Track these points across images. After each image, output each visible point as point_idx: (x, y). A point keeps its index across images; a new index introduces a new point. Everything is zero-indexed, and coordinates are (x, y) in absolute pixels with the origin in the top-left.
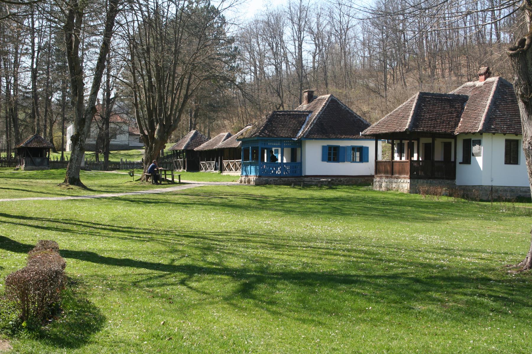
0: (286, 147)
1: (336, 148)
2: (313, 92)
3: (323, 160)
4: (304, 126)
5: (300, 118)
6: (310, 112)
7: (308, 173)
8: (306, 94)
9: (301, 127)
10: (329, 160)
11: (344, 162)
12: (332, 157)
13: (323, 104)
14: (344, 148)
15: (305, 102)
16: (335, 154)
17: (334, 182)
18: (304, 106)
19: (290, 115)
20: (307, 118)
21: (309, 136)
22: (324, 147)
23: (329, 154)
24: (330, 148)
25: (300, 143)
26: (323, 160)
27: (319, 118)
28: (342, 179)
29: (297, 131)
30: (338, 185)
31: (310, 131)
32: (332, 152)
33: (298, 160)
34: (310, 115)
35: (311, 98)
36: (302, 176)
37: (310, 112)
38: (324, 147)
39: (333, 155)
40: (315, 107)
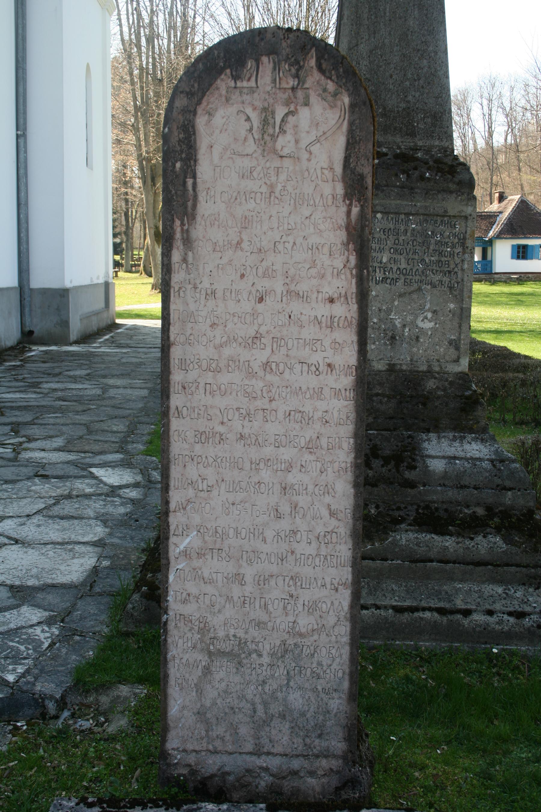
0: (478, 246)
1: (525, 247)
2: (503, 193)
3: (512, 258)
4: (494, 227)
5: (491, 218)
6: (501, 212)
7: (497, 271)
8: (497, 195)
9: (492, 227)
10: (518, 258)
11: (532, 259)
12: (521, 255)
13: (514, 205)
14: (532, 246)
15: (496, 202)
16: (523, 252)
17: (523, 278)
18: (495, 207)
19: (481, 216)
20: (498, 218)
21: (499, 236)
22: (513, 246)
23: (518, 252)
24: (519, 246)
25: (491, 242)
26: (512, 258)
27: (509, 219)
28: (530, 275)
29: (487, 231)
30: (526, 281)
31: (501, 231)
32: (521, 250)
33: (489, 258)
34: (500, 216)
35: (502, 198)
36: (492, 273)
37: (501, 212)
38: (513, 246)
39: (522, 253)
40: (505, 208)
